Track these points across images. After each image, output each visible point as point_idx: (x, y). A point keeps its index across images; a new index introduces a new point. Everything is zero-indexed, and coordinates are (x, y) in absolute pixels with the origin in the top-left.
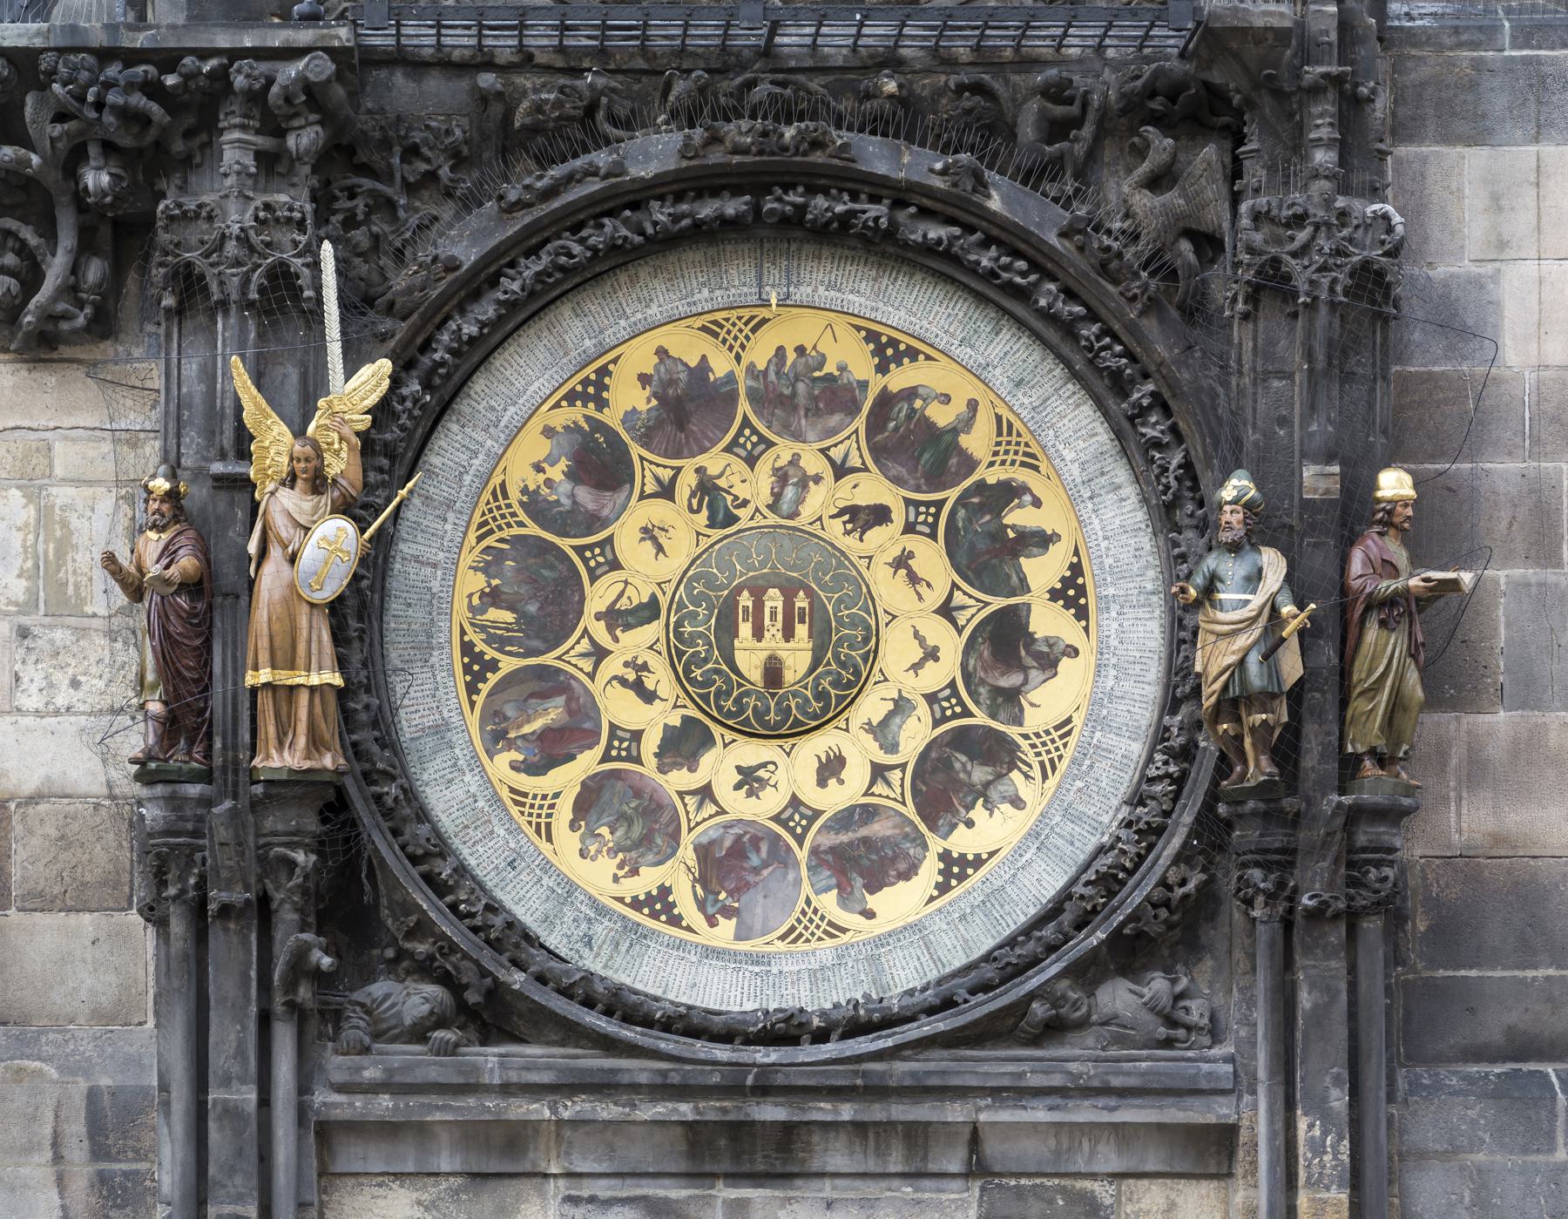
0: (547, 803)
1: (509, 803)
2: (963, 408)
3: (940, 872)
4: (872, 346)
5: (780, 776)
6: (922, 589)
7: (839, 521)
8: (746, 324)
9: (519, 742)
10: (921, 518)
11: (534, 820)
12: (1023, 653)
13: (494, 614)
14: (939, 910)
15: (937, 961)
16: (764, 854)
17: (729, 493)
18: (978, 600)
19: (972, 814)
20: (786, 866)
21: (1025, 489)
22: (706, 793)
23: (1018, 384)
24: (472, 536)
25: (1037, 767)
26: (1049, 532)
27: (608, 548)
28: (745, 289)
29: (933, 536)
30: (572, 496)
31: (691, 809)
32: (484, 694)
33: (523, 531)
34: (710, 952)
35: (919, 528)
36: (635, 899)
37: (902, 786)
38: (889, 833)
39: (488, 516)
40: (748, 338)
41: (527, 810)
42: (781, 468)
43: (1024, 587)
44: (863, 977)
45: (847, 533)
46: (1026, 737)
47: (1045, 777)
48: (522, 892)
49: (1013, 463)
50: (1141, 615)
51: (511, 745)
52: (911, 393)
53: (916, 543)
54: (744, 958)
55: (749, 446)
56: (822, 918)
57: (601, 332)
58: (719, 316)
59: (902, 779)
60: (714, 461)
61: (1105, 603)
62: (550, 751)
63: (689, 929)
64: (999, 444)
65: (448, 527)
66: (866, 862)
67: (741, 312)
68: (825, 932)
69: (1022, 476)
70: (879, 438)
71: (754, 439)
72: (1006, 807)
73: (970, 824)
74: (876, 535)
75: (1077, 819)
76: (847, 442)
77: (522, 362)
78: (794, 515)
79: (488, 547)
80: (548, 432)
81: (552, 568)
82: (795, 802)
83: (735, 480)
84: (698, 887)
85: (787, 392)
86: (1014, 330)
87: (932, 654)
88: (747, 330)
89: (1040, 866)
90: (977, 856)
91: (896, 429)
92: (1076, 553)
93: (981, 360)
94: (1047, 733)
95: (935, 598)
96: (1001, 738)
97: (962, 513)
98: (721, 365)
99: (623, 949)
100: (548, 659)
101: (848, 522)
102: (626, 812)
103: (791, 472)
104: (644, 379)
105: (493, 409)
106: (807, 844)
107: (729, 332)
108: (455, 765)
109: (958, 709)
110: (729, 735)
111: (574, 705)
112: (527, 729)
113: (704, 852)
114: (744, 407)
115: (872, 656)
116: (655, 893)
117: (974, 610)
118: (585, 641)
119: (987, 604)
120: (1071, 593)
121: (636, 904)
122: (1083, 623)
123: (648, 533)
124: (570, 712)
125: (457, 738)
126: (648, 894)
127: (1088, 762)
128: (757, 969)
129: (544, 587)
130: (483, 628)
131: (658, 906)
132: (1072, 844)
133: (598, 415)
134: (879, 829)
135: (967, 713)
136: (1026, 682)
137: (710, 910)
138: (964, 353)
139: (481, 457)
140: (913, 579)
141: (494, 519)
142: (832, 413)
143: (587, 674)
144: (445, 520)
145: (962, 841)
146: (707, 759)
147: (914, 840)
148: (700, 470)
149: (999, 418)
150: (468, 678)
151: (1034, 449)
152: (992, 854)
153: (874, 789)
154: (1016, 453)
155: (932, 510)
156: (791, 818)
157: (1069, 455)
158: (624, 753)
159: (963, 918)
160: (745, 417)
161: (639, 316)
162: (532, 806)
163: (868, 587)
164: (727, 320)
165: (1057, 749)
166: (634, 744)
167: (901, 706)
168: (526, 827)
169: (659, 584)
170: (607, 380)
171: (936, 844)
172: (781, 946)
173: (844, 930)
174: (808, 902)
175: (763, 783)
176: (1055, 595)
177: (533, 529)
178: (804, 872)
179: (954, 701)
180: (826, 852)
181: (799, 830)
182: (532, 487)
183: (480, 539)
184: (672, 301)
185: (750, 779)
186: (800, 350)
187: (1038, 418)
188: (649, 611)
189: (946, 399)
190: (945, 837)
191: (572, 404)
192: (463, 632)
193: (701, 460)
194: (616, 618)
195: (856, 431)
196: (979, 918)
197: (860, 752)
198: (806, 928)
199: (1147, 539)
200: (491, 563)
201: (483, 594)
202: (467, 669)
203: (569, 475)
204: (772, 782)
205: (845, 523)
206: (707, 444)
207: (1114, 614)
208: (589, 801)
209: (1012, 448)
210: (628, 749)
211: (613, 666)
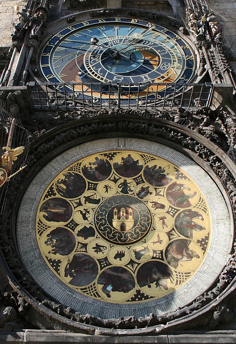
0: (46, 227)
1: (37, 222)
5: (106, 251)
6: (165, 227)
7: (152, 204)
8: (150, 158)
10: (172, 211)
11: (40, 229)
12: (184, 252)
13: (62, 185)
14: (129, 304)
16: (90, 267)
17: (129, 188)
19: (151, 284)
20: (94, 273)
21: (199, 215)
22: (85, 246)
25: (175, 280)
26: (203, 227)
27: (96, 185)
29: (173, 216)
33: (79, 173)
35: (170, 213)
37: (136, 268)
38: (126, 278)
39: (74, 167)
40: (149, 161)
46: (176, 272)
52: (181, 185)
53: (167, 215)
54: (68, 288)
56: (95, 290)
58: (146, 154)
59: (137, 267)
60: (129, 180)
63: (59, 274)
65: (64, 164)
67: (151, 155)
68: (94, 294)
69: (201, 212)
73: (150, 287)
77: (99, 144)
79: (70, 172)
80: (96, 158)
82: (106, 259)
83: (132, 186)
84: (68, 265)
87: (160, 242)
90: (147, 296)
93: (201, 184)
95: (168, 229)
97: (182, 214)
100: (68, 200)
101: (154, 205)
103: (146, 189)
104: (123, 159)
106: (103, 270)
112: (52, 210)
114: (142, 173)
116: (56, 261)
121: (50, 261)
123: (106, 187)
125: (36, 203)
128: (69, 293)
129: (76, 186)
130: (58, 186)
131: (55, 264)
133: (109, 161)
134: (124, 276)
136: (182, 259)
137: (67, 272)
139: (79, 155)
140: (164, 223)
141: (75, 168)
145: (145, 290)
146: (90, 239)
148: (125, 180)
149: (201, 198)
152: (152, 297)
153: (128, 266)
154: (202, 207)
155: (175, 211)
157: (215, 212)
159: (135, 310)
161: (128, 147)
163: (151, 220)
164: (147, 156)
168: (37, 229)
169: (102, 198)
170: (115, 155)
171: (137, 287)
173: (99, 296)
174: (94, 284)
177: (82, 174)
180: (106, 274)
183: (69, 170)
185: (98, 248)
188: (97, 202)
191: (105, 156)
192: (53, 185)
193: (126, 178)
194: (88, 200)
197: (129, 255)
200: (68, 176)
202: (48, 192)
205: (153, 205)
208: (55, 233)
209: (201, 205)
211: (81, 208)
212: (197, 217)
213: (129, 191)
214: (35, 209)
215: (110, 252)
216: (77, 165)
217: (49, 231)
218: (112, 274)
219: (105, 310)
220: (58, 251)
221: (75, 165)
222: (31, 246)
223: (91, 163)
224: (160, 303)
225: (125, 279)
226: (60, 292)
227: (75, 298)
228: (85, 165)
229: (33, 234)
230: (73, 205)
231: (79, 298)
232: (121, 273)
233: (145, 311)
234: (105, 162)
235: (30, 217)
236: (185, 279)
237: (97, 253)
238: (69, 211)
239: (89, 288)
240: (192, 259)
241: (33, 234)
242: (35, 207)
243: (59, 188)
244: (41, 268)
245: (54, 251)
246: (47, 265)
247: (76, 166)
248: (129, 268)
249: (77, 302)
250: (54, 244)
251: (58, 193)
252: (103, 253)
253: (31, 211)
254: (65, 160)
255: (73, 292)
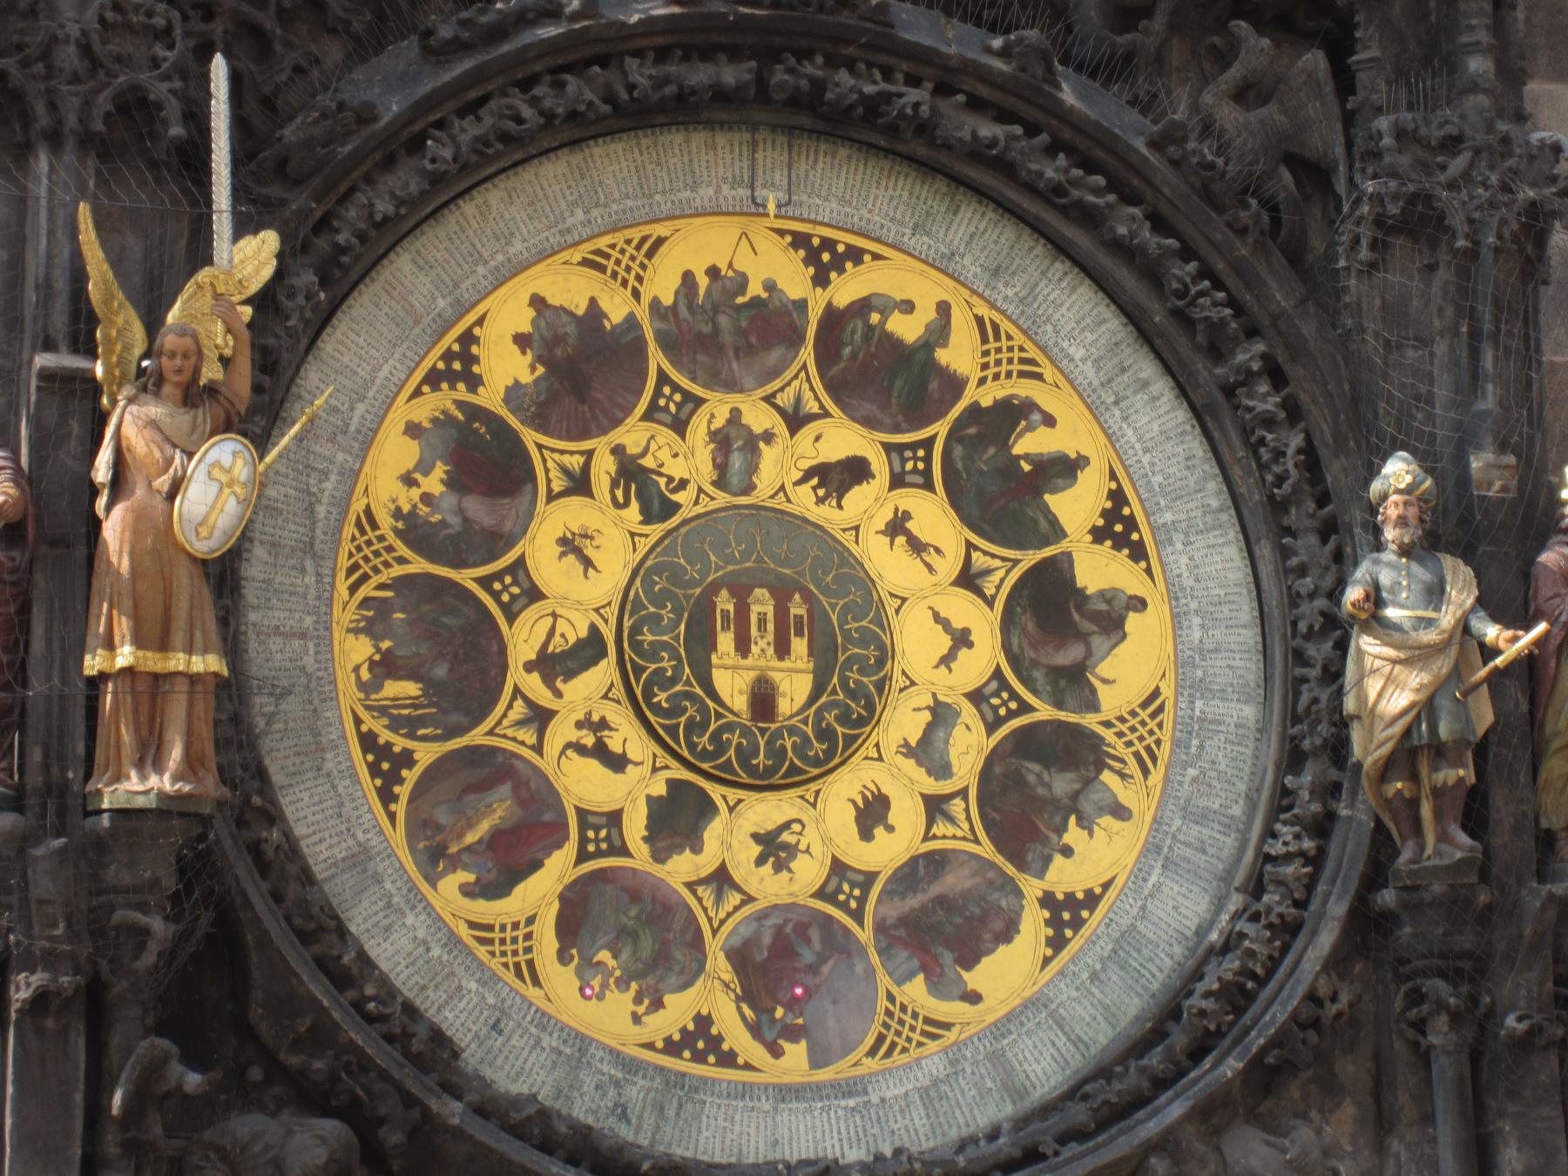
0: (520, 933)
1: (473, 943)
2: (933, 315)
3: (1048, 923)
4: (802, 253)
5: (810, 838)
6: (932, 557)
7: (806, 489)
8: (638, 248)
9: (465, 857)
11: (510, 960)
12: (1076, 617)
15: (1077, 1042)
17: (661, 474)
18: (1004, 559)
19: (1067, 838)
22: (721, 878)
23: (996, 272)
24: (342, 587)
25: (1132, 761)
26: (1073, 456)
27: (521, 573)
28: (629, 203)
29: (929, 486)
30: (461, 511)
31: (708, 903)
32: (404, 799)
34: (786, 1093)
35: (909, 479)
36: (668, 1041)
37: (969, 818)
38: (968, 884)
39: (358, 557)
40: (643, 267)
41: (497, 948)
42: (718, 431)
43: (1056, 531)
44: (989, 1084)
45: (820, 501)
46: (1107, 724)
47: (1146, 772)
48: (519, 1063)
49: (1009, 374)
50: (1212, 541)
51: (454, 864)
52: (863, 306)
53: (909, 499)
55: (673, 408)
57: (456, 286)
59: (967, 810)
60: (632, 434)
61: (1163, 534)
62: (507, 862)
63: (748, 1066)
64: (986, 353)
66: (949, 929)
67: (629, 233)
69: (1023, 389)
70: (834, 370)
71: (678, 397)
72: (1106, 821)
73: (1067, 852)
74: (859, 498)
75: (1202, 817)
76: (796, 383)
78: (749, 488)
80: (413, 430)
81: (453, 612)
82: (838, 868)
83: (664, 455)
85: (707, 329)
86: (974, 205)
87: (962, 639)
88: (640, 258)
89: (1172, 888)
90: (1089, 893)
91: (854, 356)
92: (1113, 476)
94: (1133, 714)
95: (949, 566)
96: (1077, 731)
97: (958, 451)
98: (617, 308)
99: (671, 1112)
100: (477, 736)
101: (819, 486)
102: (626, 925)
103: (733, 433)
104: (522, 341)
105: (336, 410)
106: (869, 920)
107: (618, 262)
108: (389, 905)
109: (1013, 705)
110: (733, 794)
111: (524, 793)
112: (471, 838)
113: (739, 957)
114: (656, 358)
115: (885, 655)
116: (691, 1027)
117: (1001, 573)
118: (519, 703)
119: (1016, 562)
120: (1116, 528)
121: (672, 1048)
122: (1143, 564)
123: (570, 545)
124: (522, 803)
126: (684, 1030)
127: (1195, 742)
128: (851, 1103)
130: (383, 711)
131: (701, 1045)
132: (1204, 852)
134: (954, 881)
135: (1025, 708)
137: (769, 1036)
138: (920, 243)
139: (333, 477)
140: (917, 546)
141: (366, 559)
142: (768, 346)
143: (532, 748)
144: (303, 570)
145: (1065, 876)
146: (713, 832)
147: (1003, 887)
148: (618, 451)
149: (980, 321)
150: (378, 782)
151: (1033, 352)
152: (1106, 886)
155: (921, 453)
156: (839, 890)
157: (1078, 353)
158: (604, 846)
159: (1094, 977)
160: (660, 371)
162: (503, 942)
164: (613, 246)
165: (1151, 733)
166: (614, 832)
167: (941, 715)
168: (501, 971)
169: (597, 610)
171: (1032, 887)
172: (872, 1064)
173: (947, 1026)
174: (891, 998)
175: (792, 850)
176: (1098, 535)
177: (419, 565)
178: (875, 958)
179: (1005, 695)
180: (895, 926)
181: (853, 904)
182: (406, 508)
183: (353, 589)
184: (539, 232)
186: (713, 272)
187: (1029, 311)
188: (589, 650)
189: (908, 307)
190: (1041, 875)
191: (436, 387)
192: (358, 721)
193: (618, 436)
194: (556, 665)
195: (804, 367)
196: (1114, 974)
197: (906, 787)
198: (898, 1033)
199: (1196, 443)
200: (374, 622)
201: (373, 665)
202: (374, 770)
203: (451, 483)
204: (802, 846)
205: (814, 489)
206: (619, 414)
207: (1179, 546)
209: (1004, 356)
210: (608, 839)
211: (562, 732)
212: (1023, 423)
213: (675, 490)
214: (411, 896)
215: (825, 820)
216: (363, 532)
217: (547, 941)
218: (912, 910)
219: (1009, 1055)
220: (660, 986)
221: (354, 539)
222: (554, 1057)
223: (409, 473)
224: (1150, 885)
225: (969, 890)
226: (818, 1124)
227: (883, 1100)
228: (392, 507)
229: (508, 1003)
230: (522, 743)
231: (896, 1092)
232: (936, 878)
233: (1127, 953)
234: (460, 416)
235: (425, 942)
236: (1156, 729)
237: (790, 871)
238: (533, 784)
239: (886, 1026)
240: (1122, 627)
241: (508, 1003)
242: (399, 884)
243: (395, 712)
244: (675, 1105)
245: (646, 1002)
246: (684, 1075)
247: (361, 540)
248: (944, 837)
249: (902, 1111)
250: (618, 973)
251: (412, 736)
252: (807, 851)
253: (404, 915)
254: (293, 550)
255: (859, 1088)
